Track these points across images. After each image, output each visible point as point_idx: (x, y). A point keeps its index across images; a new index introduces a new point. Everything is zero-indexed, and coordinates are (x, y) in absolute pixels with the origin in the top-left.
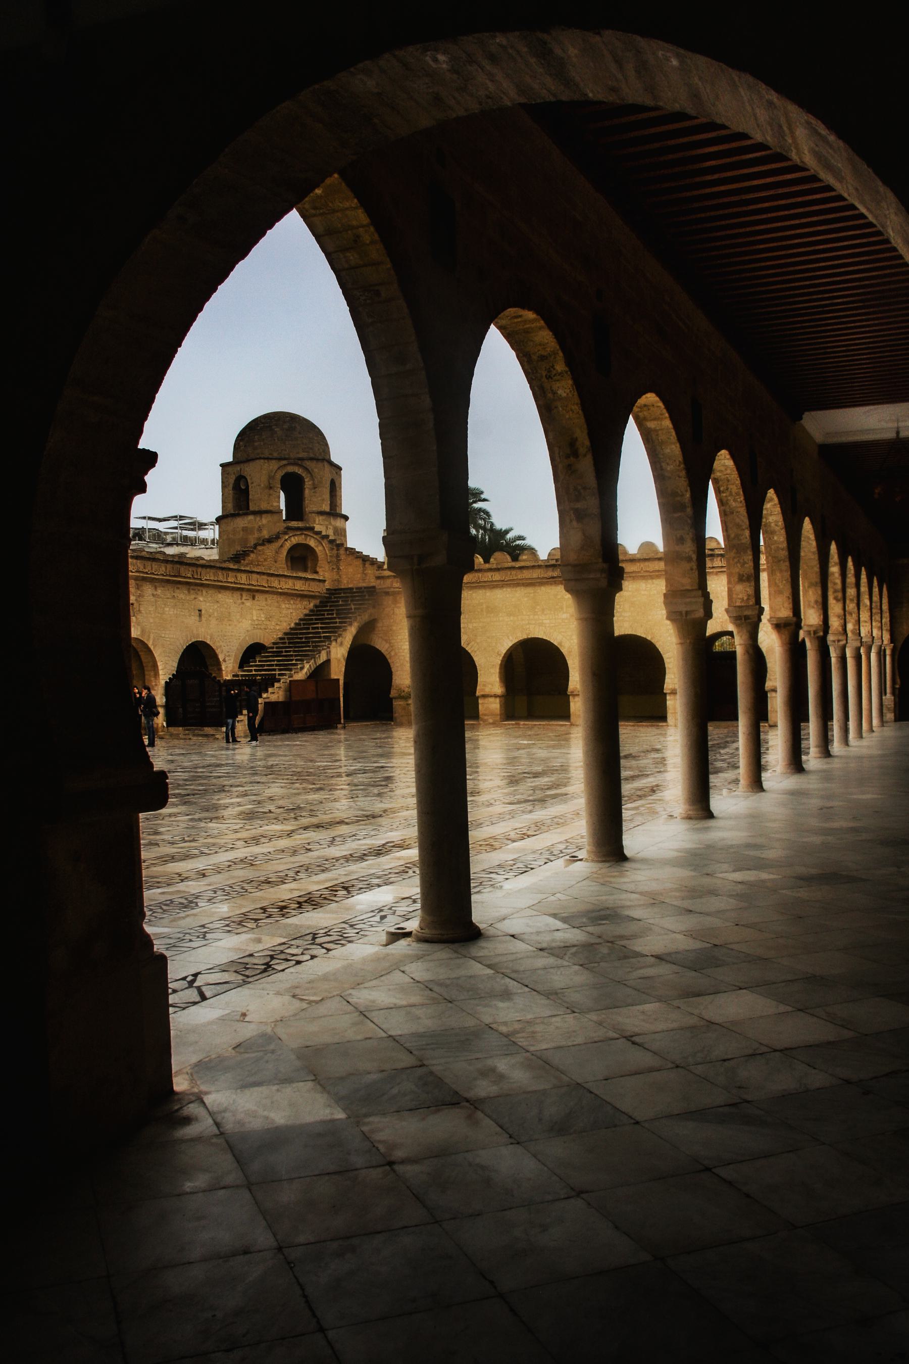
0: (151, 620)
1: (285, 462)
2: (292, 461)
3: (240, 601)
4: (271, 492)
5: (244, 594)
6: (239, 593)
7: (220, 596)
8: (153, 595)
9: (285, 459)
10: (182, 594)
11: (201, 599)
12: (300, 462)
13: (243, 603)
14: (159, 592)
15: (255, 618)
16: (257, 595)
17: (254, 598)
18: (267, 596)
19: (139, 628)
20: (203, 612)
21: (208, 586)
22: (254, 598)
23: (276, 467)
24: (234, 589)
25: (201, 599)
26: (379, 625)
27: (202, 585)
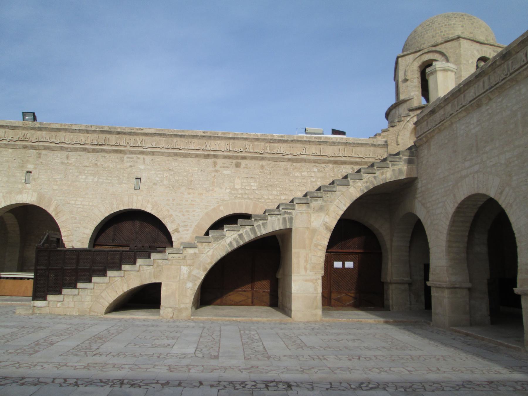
0: (55, 187)
1: (419, 54)
2: (426, 51)
3: (211, 169)
4: (408, 83)
5: (220, 162)
6: (210, 161)
7: (175, 164)
8: (62, 163)
9: (420, 51)
10: (109, 161)
11: (142, 167)
12: (434, 49)
13: (217, 171)
14: (72, 160)
15: (237, 187)
16: (243, 162)
17: (238, 165)
18: (261, 163)
19: (35, 194)
20: (143, 180)
21: (153, 153)
22: (238, 165)
23: (412, 60)
24: (197, 156)
25: (142, 167)
26: (419, 185)
27: (142, 153)
